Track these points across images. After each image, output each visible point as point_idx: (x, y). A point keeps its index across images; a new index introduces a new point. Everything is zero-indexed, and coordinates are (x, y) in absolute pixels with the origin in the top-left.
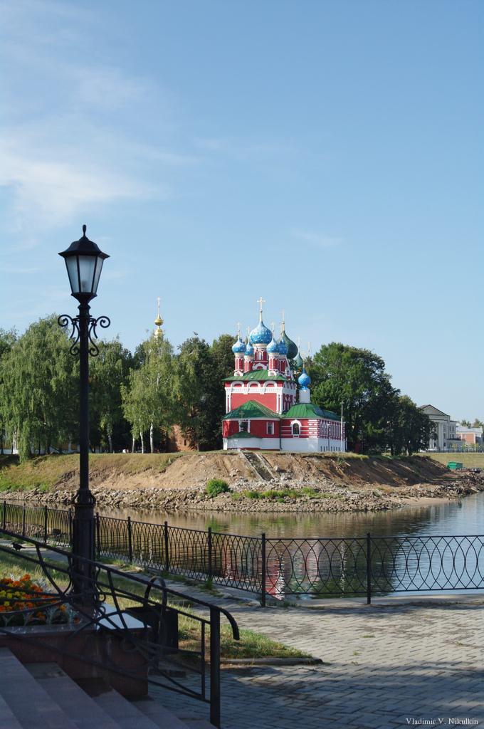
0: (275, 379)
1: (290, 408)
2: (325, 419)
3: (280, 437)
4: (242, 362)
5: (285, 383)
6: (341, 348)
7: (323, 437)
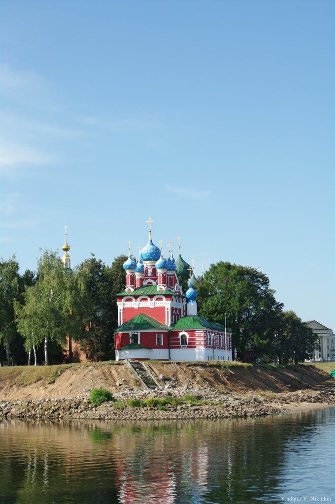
0: (164, 293)
1: (178, 319)
2: (211, 330)
3: (169, 348)
4: (133, 279)
5: (173, 297)
6: (229, 267)
7: (209, 347)
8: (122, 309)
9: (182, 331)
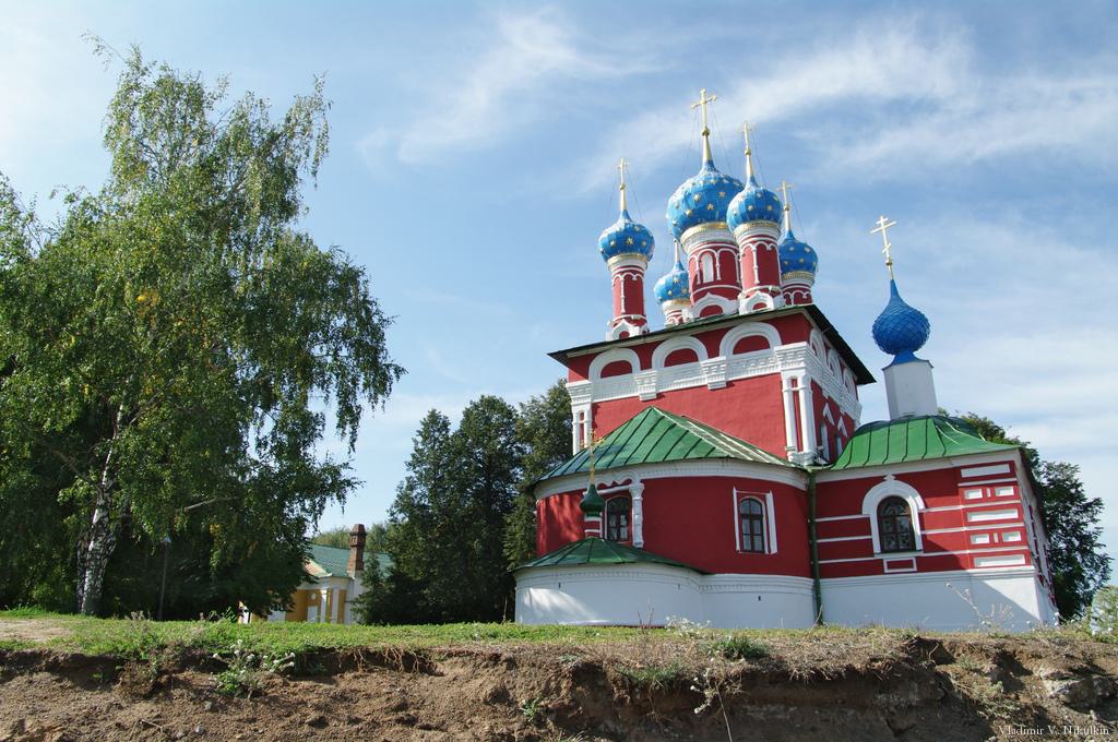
3: (816, 573)
8: (587, 409)
9: (880, 479)
